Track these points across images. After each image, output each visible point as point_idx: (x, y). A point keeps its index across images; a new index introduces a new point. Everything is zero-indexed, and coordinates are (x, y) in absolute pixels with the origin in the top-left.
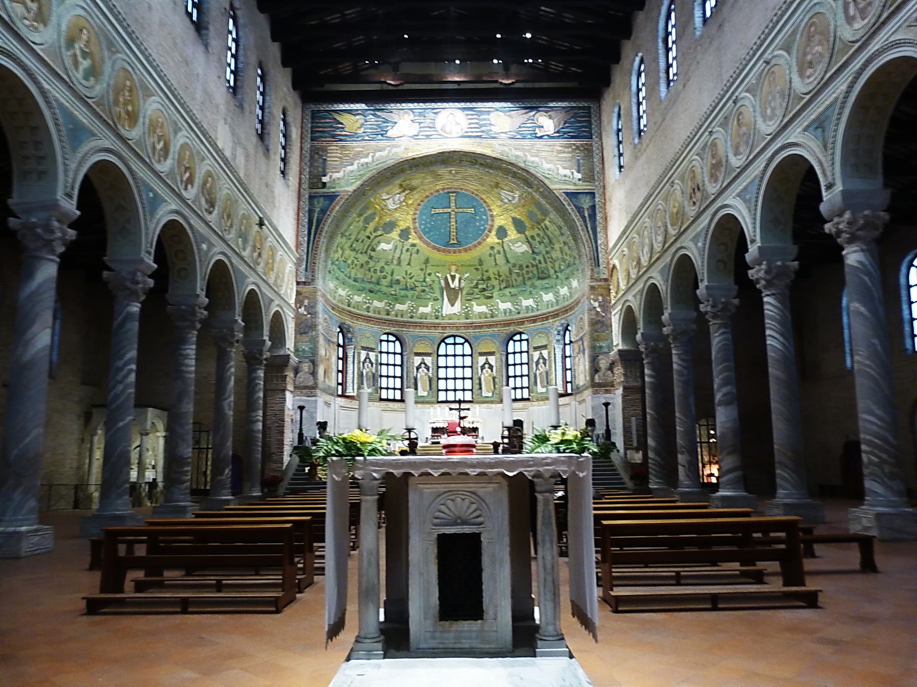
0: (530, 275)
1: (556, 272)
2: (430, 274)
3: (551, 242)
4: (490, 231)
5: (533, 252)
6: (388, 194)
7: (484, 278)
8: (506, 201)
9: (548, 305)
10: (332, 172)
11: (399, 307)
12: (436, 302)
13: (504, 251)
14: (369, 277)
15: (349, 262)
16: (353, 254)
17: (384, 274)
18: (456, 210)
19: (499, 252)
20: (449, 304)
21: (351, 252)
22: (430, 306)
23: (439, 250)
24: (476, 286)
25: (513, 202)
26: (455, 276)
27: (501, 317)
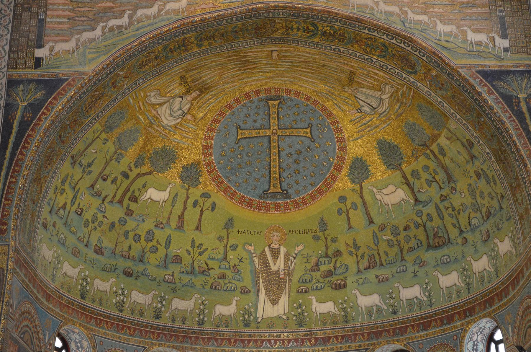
0: (413, 243)
1: (461, 231)
2: (234, 247)
3: (450, 178)
4: (338, 169)
5: (416, 200)
6: (159, 94)
7: (330, 252)
8: (367, 109)
9: (450, 295)
10: (56, 42)
11: (178, 304)
12: (244, 296)
13: (364, 204)
14: (126, 249)
15: (88, 216)
16: (96, 202)
17: (154, 243)
18: (279, 133)
19: (354, 206)
20: (267, 300)
21: (92, 199)
22: (234, 302)
23: (249, 204)
24: (316, 267)
25: (380, 110)
26: (279, 250)
27: (362, 321)
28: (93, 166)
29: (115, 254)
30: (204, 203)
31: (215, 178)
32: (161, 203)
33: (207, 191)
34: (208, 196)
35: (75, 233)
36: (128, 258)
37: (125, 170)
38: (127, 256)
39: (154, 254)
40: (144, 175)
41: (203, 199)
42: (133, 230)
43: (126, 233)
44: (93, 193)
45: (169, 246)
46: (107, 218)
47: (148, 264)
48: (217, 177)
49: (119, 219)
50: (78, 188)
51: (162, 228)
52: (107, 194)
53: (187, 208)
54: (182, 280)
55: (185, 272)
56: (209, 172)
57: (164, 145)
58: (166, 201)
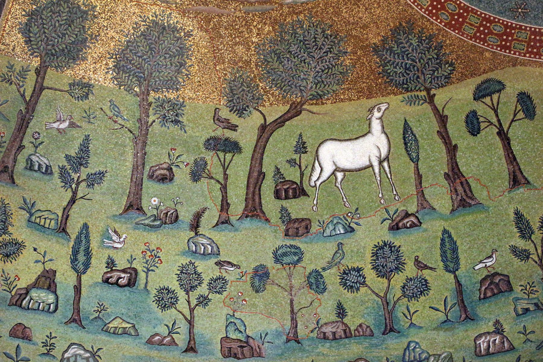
17: (410, 270)
28: (93, 160)
29: (299, 343)
30: (496, 111)
31: (482, 33)
32: (377, 170)
33: (484, 77)
34: (497, 88)
35: (133, 332)
36: (346, 337)
37: (213, 134)
38: (340, 332)
39: (422, 298)
40: (280, 122)
41: (487, 100)
42: (330, 265)
43: (313, 280)
44: (146, 222)
45: (456, 260)
46: (233, 265)
47: (413, 330)
48: (485, 27)
49: (275, 253)
50: (79, 225)
51: (413, 225)
52: (195, 209)
53: (456, 146)
54: (533, 332)
55: (532, 307)
56: (458, 27)
57: (281, 26)
58: (387, 158)
